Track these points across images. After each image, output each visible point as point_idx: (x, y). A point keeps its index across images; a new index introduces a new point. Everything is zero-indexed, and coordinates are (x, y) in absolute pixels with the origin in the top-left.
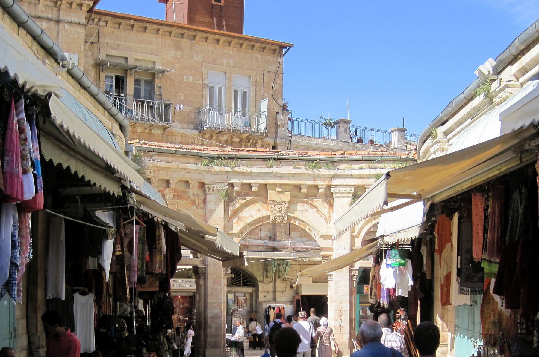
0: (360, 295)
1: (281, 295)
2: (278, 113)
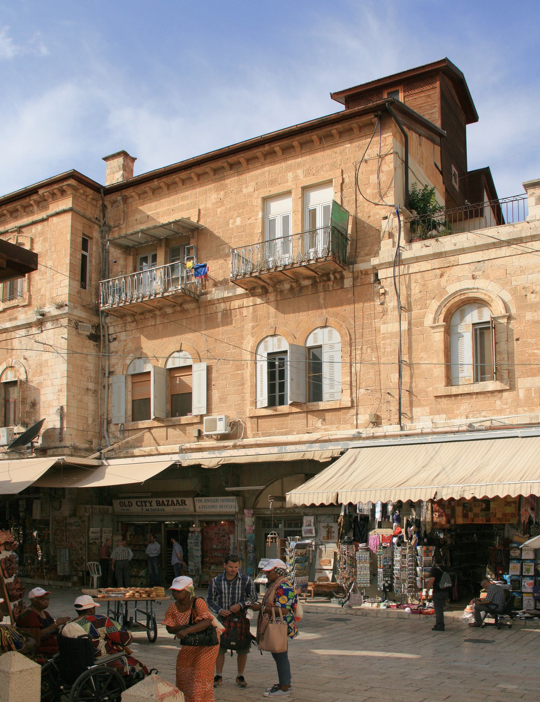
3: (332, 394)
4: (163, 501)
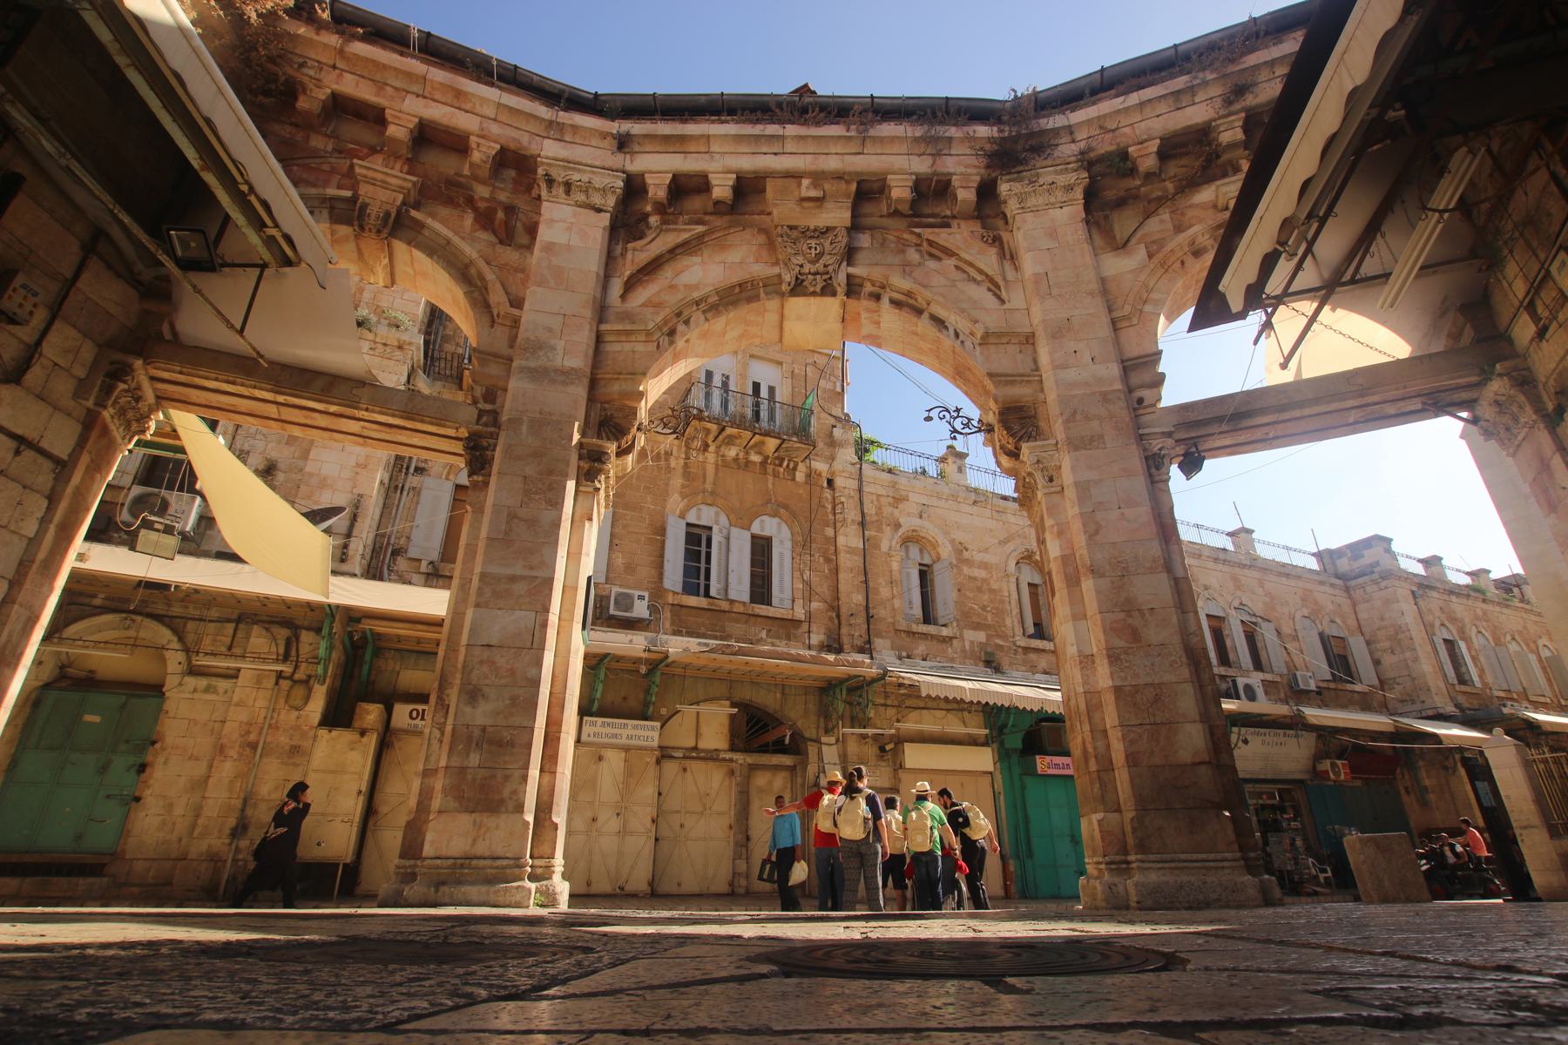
2: (834, 426)
3: (782, 600)
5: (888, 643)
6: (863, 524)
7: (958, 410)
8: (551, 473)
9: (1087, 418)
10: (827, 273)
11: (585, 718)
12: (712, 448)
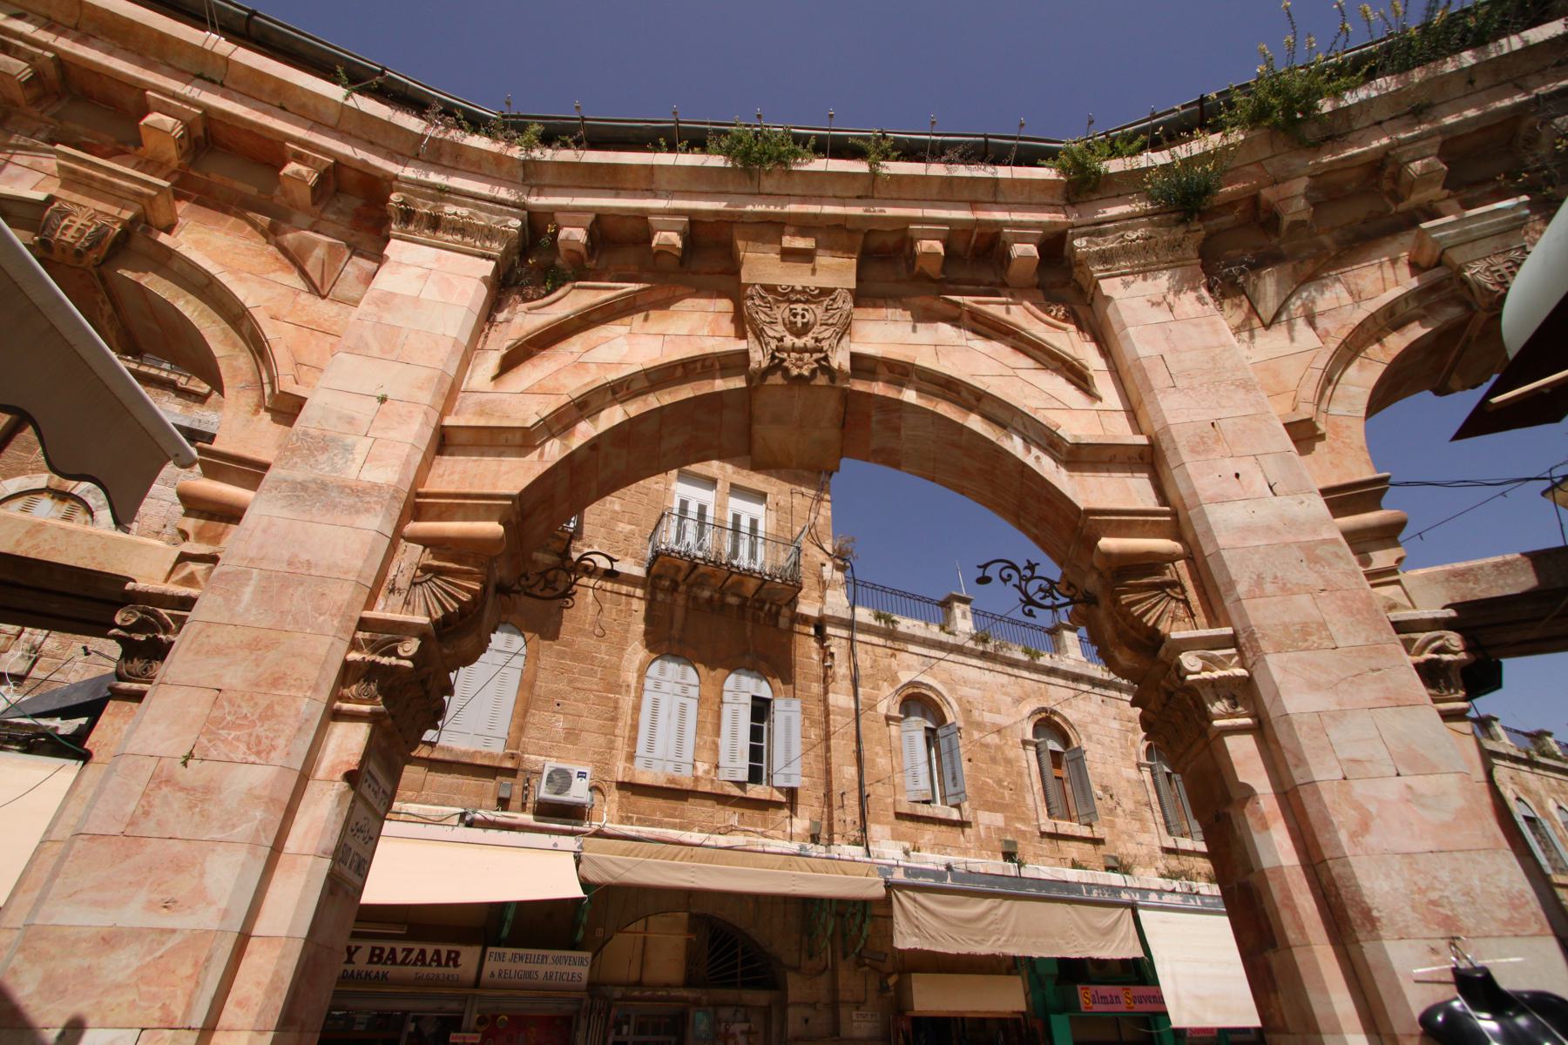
0: (1070, 1017)
1: (854, 1018)
2: (823, 565)
4: (393, 951)
5: (887, 830)
6: (855, 682)
7: (1031, 567)
8: (276, 681)
9: (1286, 589)
10: (821, 350)
11: (490, 949)
12: (682, 588)
